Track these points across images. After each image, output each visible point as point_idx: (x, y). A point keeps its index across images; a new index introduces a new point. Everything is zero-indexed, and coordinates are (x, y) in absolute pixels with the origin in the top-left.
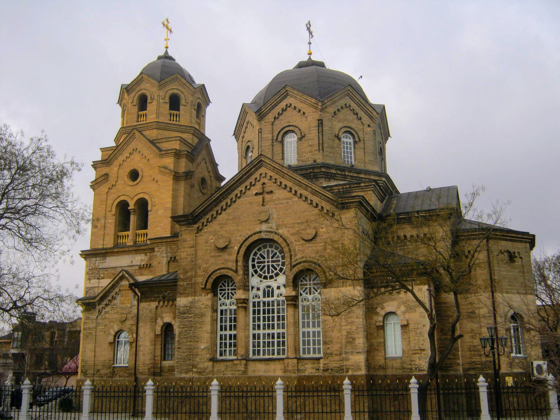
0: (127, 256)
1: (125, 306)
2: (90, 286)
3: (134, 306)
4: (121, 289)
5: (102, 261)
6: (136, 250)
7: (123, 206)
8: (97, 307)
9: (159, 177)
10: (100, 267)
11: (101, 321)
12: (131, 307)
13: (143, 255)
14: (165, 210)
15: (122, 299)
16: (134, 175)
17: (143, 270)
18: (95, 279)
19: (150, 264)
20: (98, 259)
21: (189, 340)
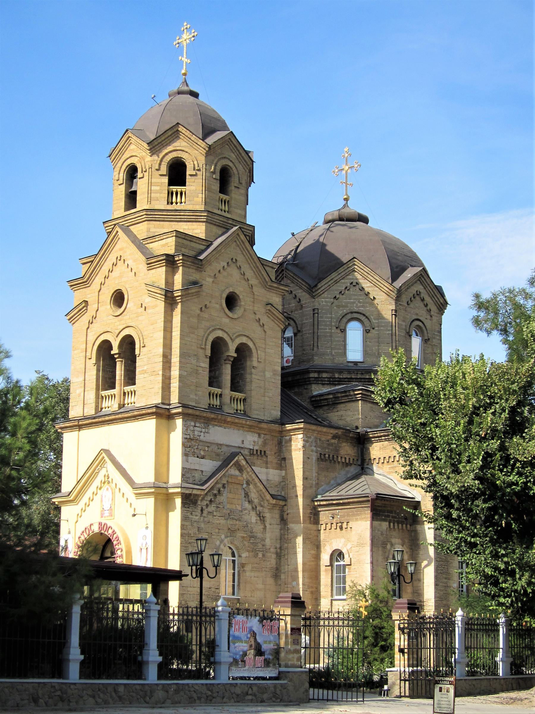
0: (236, 431)
1: (234, 507)
2: (188, 466)
3: (245, 509)
4: (230, 480)
5: (203, 430)
6: (251, 427)
7: (218, 346)
8: (199, 503)
9: (265, 320)
10: (202, 438)
11: (202, 525)
12: (242, 511)
13: (257, 435)
14: (274, 374)
15: (231, 496)
16: (231, 301)
17: (255, 457)
18: (194, 455)
19: (265, 452)
20: (197, 425)
21: (444, 576)
